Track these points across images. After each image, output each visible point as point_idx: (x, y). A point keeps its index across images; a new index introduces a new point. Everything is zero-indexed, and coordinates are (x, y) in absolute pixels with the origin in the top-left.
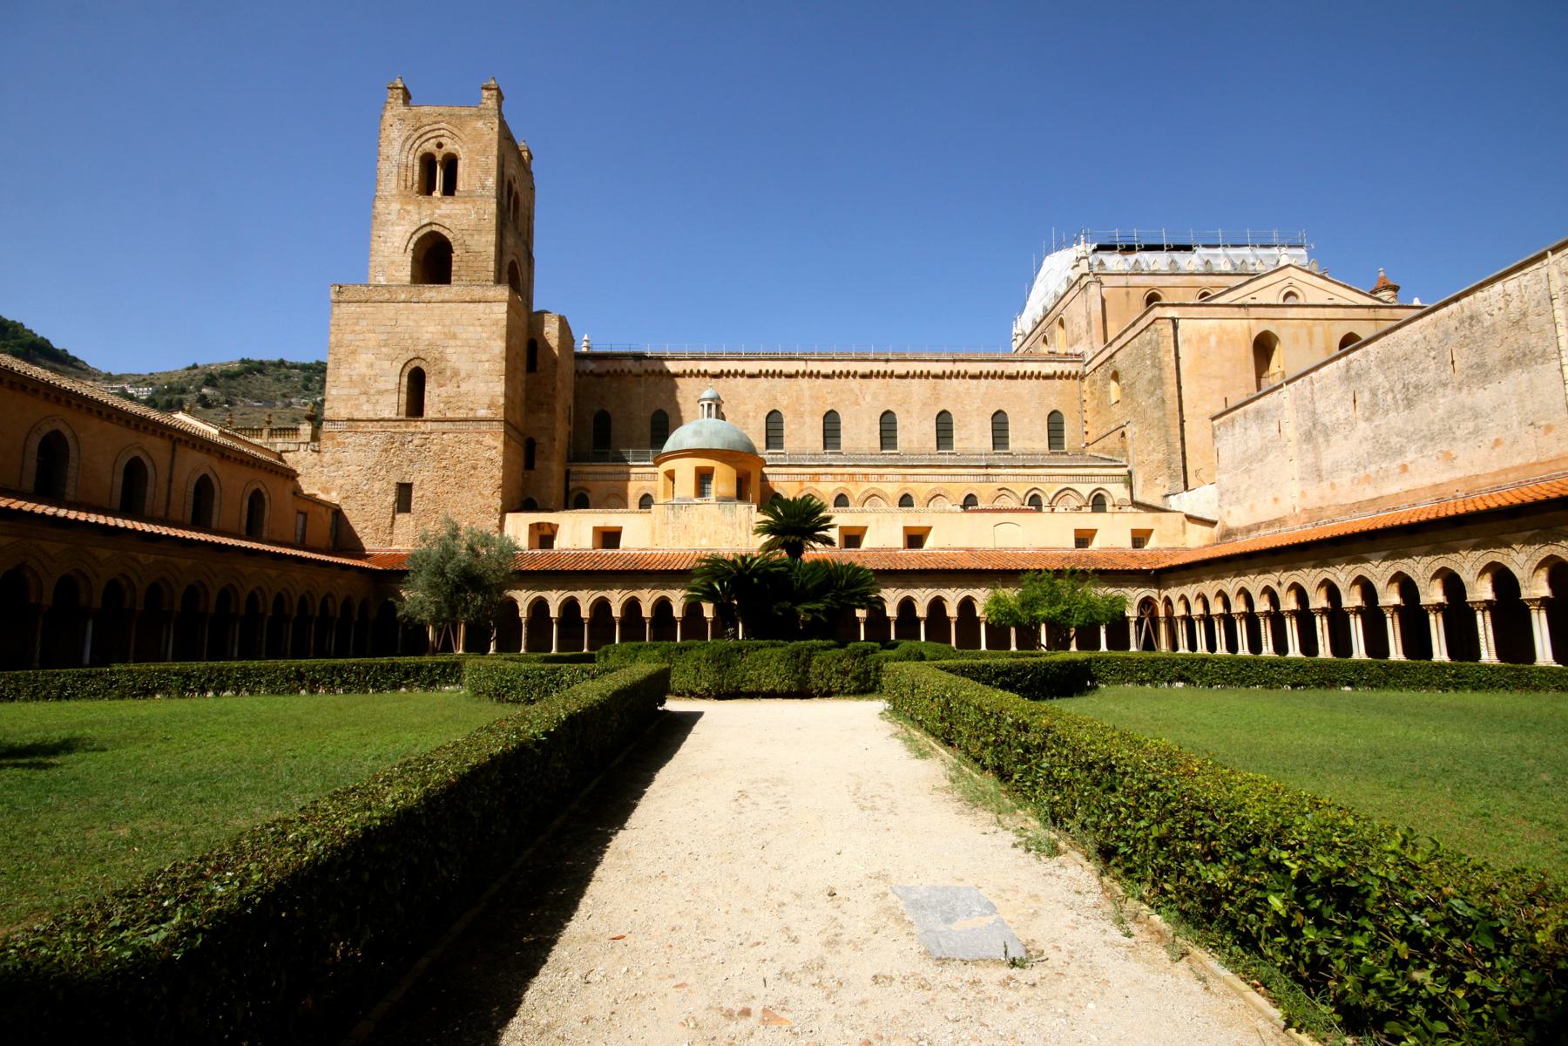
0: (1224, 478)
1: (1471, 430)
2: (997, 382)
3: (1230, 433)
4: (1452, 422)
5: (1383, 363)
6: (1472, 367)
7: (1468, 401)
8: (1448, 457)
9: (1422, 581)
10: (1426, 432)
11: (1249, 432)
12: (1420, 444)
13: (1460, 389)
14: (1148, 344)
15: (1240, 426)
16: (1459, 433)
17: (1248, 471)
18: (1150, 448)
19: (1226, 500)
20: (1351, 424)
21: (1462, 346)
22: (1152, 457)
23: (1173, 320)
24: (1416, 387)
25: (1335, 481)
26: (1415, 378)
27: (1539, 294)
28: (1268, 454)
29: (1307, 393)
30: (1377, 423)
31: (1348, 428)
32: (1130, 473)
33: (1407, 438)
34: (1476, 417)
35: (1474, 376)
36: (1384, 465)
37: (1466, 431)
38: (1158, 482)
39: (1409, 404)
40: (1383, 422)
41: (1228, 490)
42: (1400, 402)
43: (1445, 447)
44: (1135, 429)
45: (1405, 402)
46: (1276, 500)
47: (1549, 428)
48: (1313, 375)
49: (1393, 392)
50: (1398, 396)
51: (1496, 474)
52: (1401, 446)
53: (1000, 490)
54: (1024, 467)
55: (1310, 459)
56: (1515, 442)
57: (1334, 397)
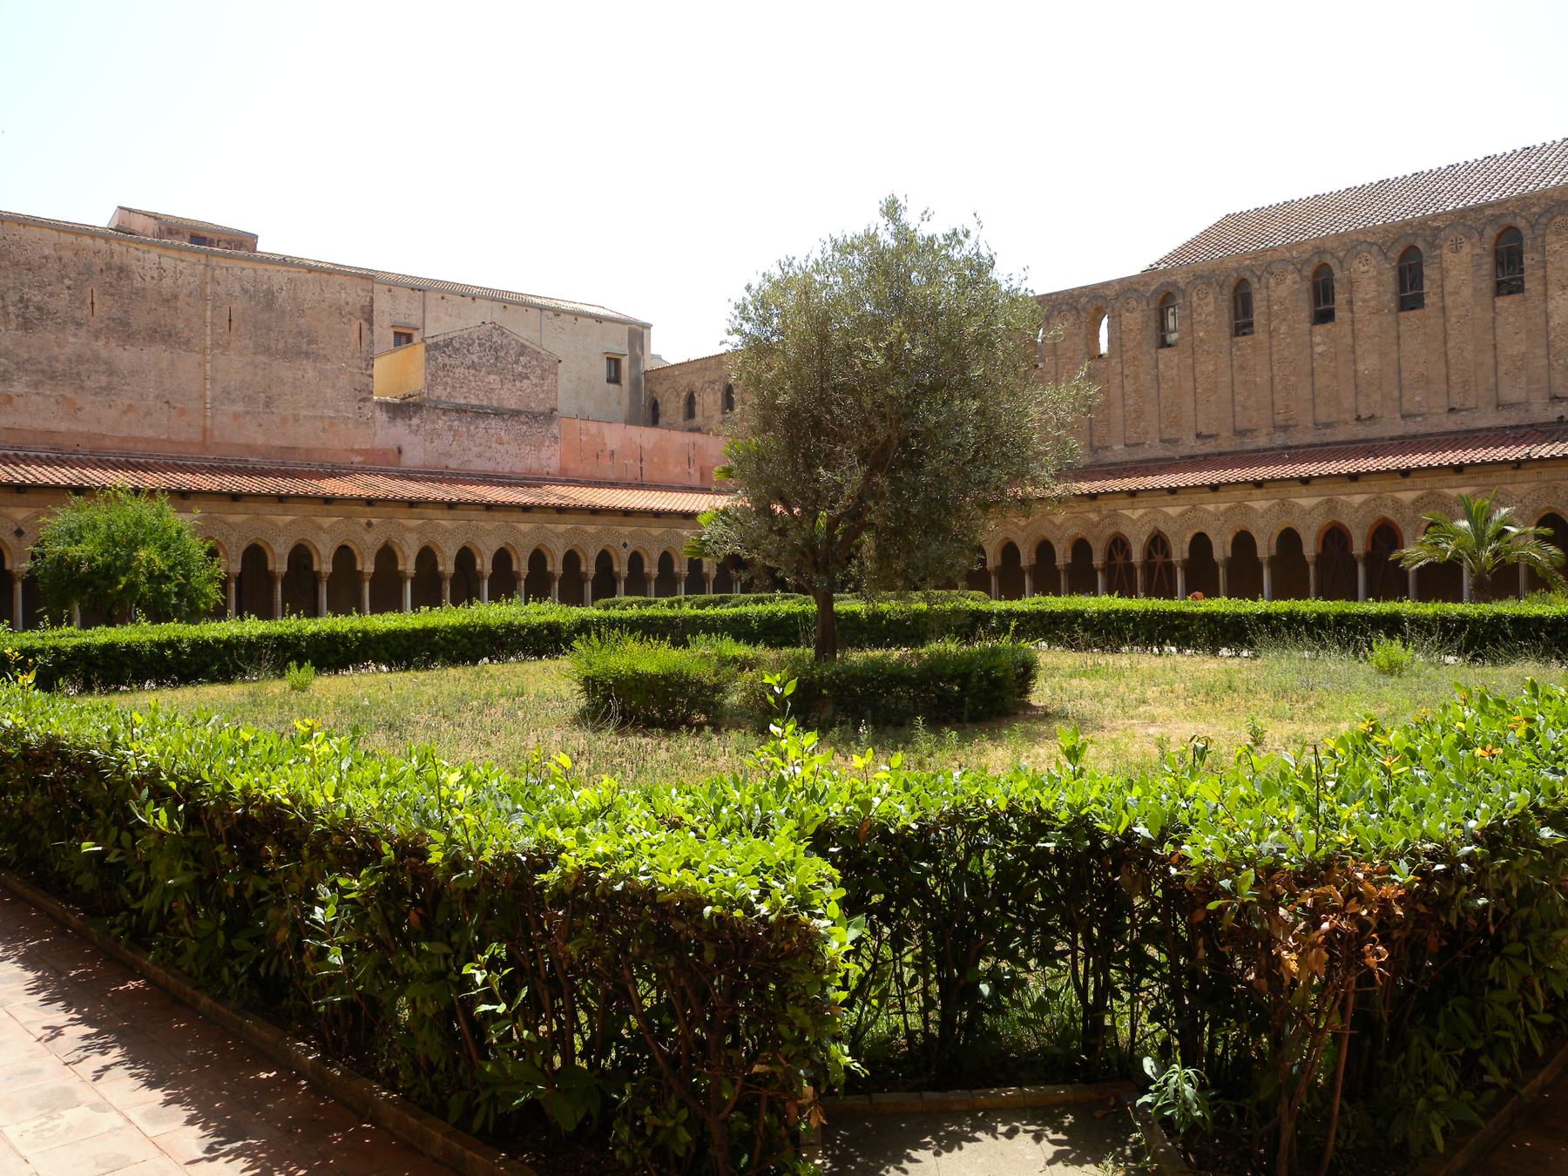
1: (104, 384)
6: (114, 320)
7: (104, 354)
10: (46, 368)
12: (35, 377)
16: (87, 383)
21: (105, 293)
24: (39, 309)
33: (17, 363)
34: (111, 374)
39: (26, 325)
47: (182, 412)
51: (124, 439)
56: (148, 414)
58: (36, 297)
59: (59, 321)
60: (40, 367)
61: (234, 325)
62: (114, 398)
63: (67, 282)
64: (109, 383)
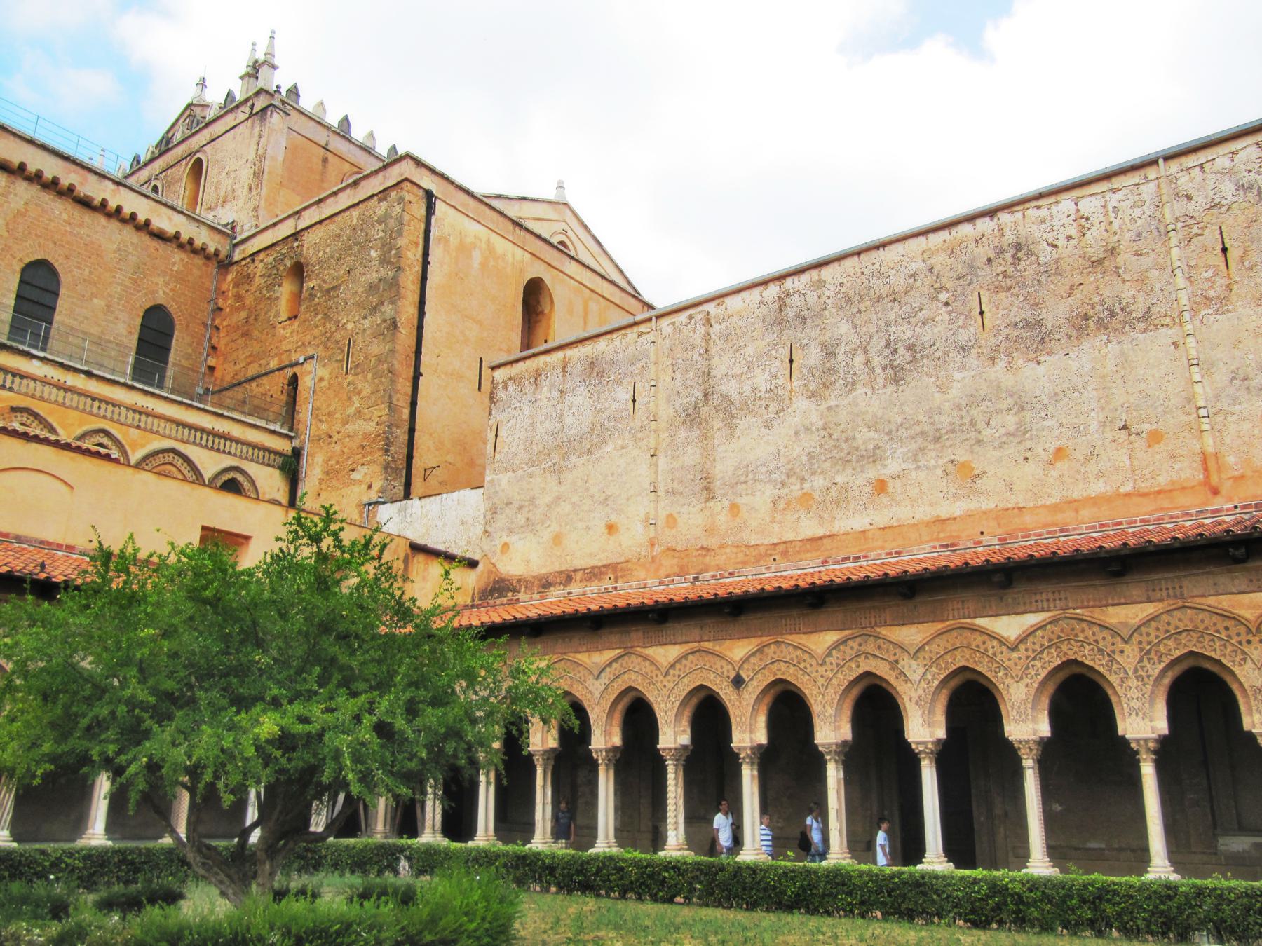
0: (504, 478)
1: (1012, 429)
2: (47, 198)
3: (529, 397)
4: (974, 412)
5: (849, 301)
7: (1008, 380)
8: (967, 475)
9: (1133, 682)
10: (927, 428)
11: (568, 398)
13: (993, 359)
14: (379, 222)
15: (553, 385)
16: (987, 432)
17: (556, 470)
18: (351, 411)
19: (502, 520)
20: (778, 400)
21: (998, 289)
22: (350, 428)
23: (429, 196)
24: (910, 348)
25: (739, 500)
26: (909, 333)
27: (1139, 222)
28: (604, 441)
29: (697, 339)
30: (832, 403)
31: (774, 407)
32: (297, 453)
34: (1022, 409)
35: (1018, 339)
36: (839, 479)
37: (1002, 431)
38: (355, 476)
39: (896, 375)
40: (845, 402)
41: (509, 504)
42: (879, 370)
43: (962, 456)
44: (322, 372)
45: (889, 371)
46: (611, 528)
48: (710, 307)
49: (866, 351)
50: (876, 361)
51: (1055, 508)
52: (877, 447)
53: (14, 410)
54: (89, 374)
55: (691, 456)
56: (1092, 455)
57: (750, 351)
58: (904, 333)
59: (937, 355)
60: (918, 429)
61: (1233, 254)
62: (1028, 444)
63: (943, 296)
64: (1020, 423)
